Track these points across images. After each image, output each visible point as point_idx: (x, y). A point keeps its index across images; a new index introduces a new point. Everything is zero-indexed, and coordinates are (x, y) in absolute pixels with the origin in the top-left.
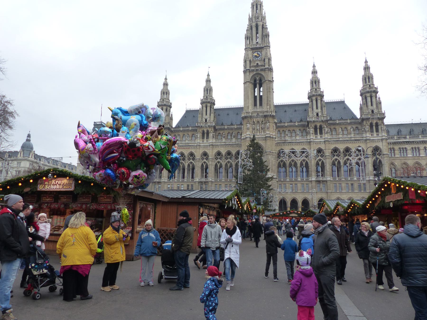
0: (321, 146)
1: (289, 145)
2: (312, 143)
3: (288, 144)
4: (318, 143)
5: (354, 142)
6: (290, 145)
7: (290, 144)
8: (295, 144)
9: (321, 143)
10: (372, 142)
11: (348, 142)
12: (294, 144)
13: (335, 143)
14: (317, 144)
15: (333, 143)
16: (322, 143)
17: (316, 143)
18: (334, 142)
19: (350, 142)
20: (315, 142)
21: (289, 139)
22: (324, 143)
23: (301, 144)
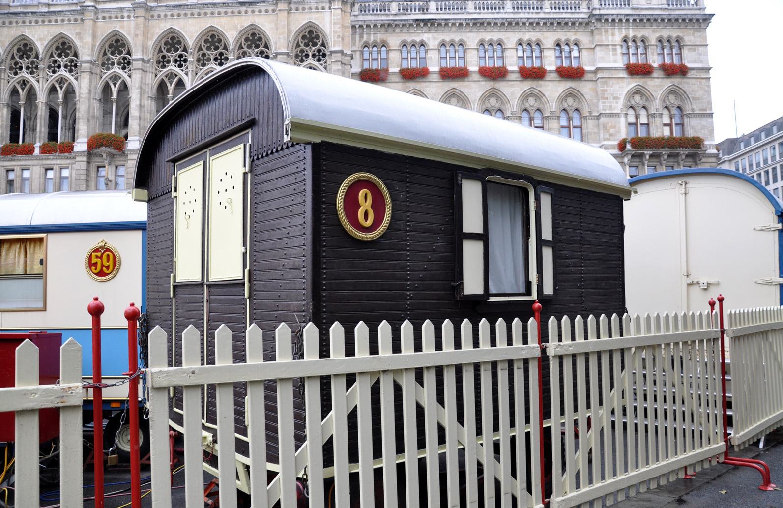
0: (122, 27)
1: (11, 23)
2: (89, 15)
3: (7, 21)
4: (113, 16)
5: (236, 10)
6: (17, 23)
7: (14, 19)
8: (34, 19)
9: (122, 17)
10: (297, 9)
11: (216, 11)
12: (30, 22)
13: (172, 15)
14: (110, 18)
15: (166, 16)
16: (126, 15)
17: (107, 15)
18: (169, 13)
19: (222, 10)
20: (103, 11)
21: (15, 4)
22: (132, 15)
23: (56, 21)
